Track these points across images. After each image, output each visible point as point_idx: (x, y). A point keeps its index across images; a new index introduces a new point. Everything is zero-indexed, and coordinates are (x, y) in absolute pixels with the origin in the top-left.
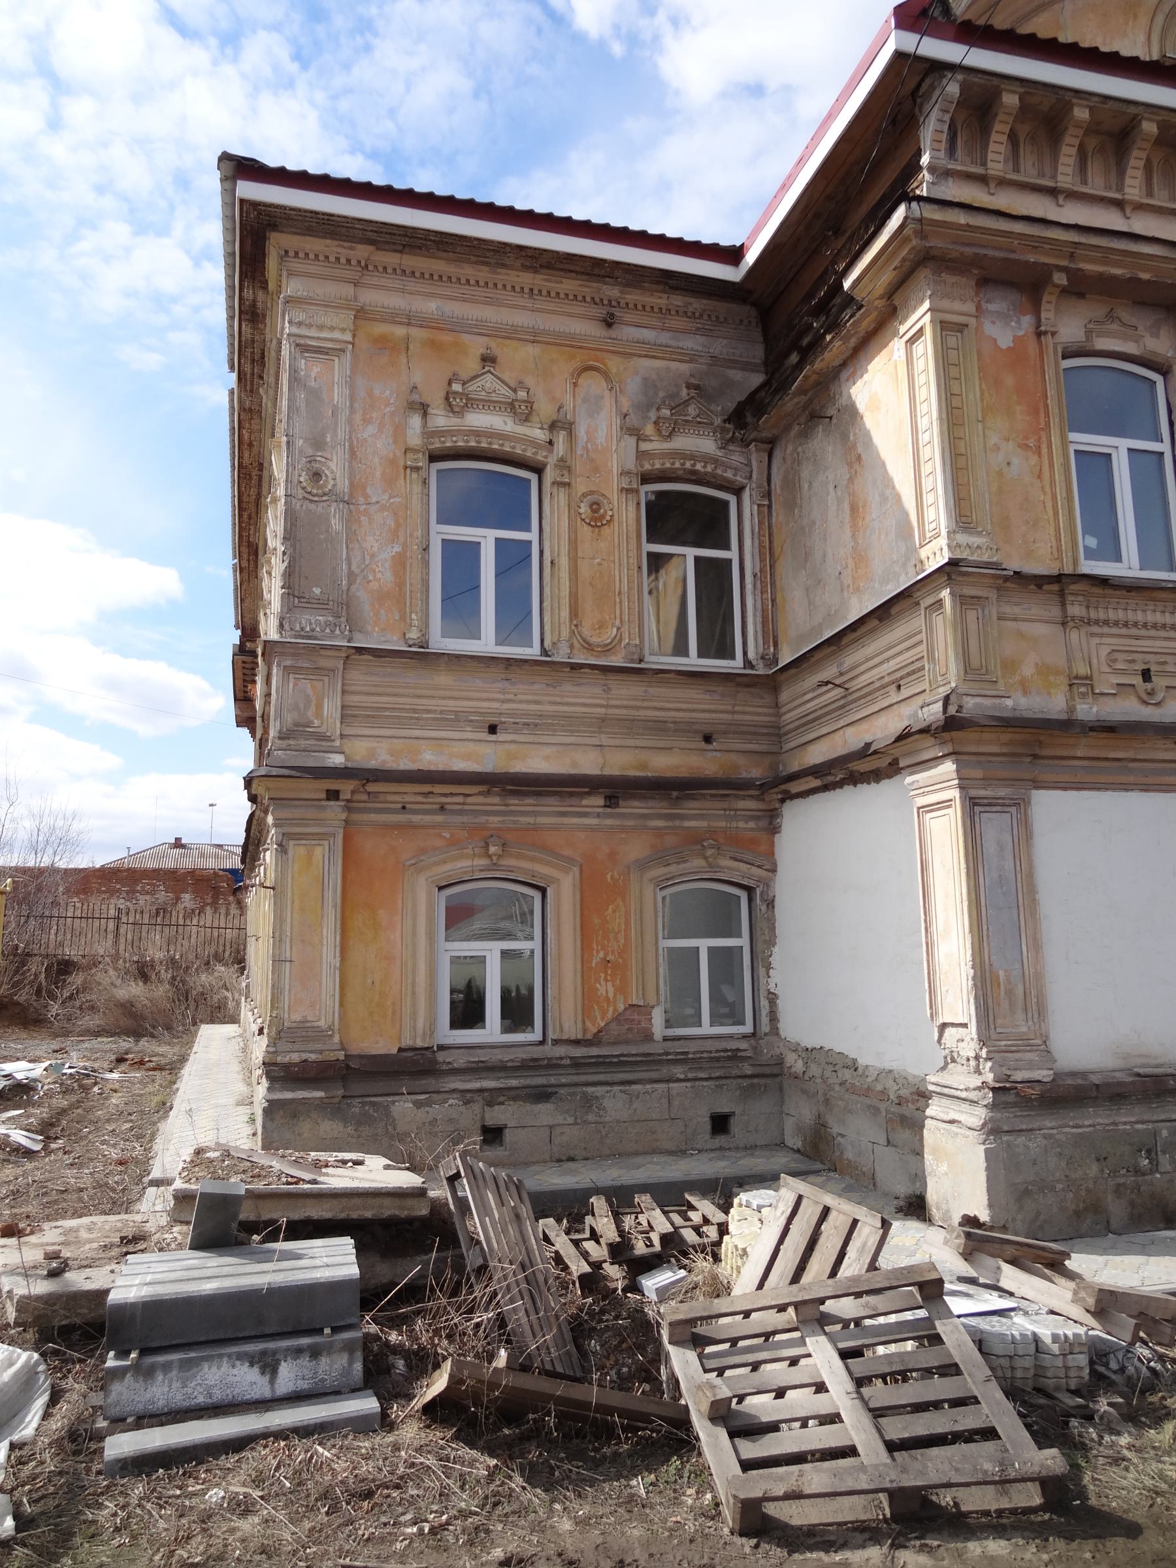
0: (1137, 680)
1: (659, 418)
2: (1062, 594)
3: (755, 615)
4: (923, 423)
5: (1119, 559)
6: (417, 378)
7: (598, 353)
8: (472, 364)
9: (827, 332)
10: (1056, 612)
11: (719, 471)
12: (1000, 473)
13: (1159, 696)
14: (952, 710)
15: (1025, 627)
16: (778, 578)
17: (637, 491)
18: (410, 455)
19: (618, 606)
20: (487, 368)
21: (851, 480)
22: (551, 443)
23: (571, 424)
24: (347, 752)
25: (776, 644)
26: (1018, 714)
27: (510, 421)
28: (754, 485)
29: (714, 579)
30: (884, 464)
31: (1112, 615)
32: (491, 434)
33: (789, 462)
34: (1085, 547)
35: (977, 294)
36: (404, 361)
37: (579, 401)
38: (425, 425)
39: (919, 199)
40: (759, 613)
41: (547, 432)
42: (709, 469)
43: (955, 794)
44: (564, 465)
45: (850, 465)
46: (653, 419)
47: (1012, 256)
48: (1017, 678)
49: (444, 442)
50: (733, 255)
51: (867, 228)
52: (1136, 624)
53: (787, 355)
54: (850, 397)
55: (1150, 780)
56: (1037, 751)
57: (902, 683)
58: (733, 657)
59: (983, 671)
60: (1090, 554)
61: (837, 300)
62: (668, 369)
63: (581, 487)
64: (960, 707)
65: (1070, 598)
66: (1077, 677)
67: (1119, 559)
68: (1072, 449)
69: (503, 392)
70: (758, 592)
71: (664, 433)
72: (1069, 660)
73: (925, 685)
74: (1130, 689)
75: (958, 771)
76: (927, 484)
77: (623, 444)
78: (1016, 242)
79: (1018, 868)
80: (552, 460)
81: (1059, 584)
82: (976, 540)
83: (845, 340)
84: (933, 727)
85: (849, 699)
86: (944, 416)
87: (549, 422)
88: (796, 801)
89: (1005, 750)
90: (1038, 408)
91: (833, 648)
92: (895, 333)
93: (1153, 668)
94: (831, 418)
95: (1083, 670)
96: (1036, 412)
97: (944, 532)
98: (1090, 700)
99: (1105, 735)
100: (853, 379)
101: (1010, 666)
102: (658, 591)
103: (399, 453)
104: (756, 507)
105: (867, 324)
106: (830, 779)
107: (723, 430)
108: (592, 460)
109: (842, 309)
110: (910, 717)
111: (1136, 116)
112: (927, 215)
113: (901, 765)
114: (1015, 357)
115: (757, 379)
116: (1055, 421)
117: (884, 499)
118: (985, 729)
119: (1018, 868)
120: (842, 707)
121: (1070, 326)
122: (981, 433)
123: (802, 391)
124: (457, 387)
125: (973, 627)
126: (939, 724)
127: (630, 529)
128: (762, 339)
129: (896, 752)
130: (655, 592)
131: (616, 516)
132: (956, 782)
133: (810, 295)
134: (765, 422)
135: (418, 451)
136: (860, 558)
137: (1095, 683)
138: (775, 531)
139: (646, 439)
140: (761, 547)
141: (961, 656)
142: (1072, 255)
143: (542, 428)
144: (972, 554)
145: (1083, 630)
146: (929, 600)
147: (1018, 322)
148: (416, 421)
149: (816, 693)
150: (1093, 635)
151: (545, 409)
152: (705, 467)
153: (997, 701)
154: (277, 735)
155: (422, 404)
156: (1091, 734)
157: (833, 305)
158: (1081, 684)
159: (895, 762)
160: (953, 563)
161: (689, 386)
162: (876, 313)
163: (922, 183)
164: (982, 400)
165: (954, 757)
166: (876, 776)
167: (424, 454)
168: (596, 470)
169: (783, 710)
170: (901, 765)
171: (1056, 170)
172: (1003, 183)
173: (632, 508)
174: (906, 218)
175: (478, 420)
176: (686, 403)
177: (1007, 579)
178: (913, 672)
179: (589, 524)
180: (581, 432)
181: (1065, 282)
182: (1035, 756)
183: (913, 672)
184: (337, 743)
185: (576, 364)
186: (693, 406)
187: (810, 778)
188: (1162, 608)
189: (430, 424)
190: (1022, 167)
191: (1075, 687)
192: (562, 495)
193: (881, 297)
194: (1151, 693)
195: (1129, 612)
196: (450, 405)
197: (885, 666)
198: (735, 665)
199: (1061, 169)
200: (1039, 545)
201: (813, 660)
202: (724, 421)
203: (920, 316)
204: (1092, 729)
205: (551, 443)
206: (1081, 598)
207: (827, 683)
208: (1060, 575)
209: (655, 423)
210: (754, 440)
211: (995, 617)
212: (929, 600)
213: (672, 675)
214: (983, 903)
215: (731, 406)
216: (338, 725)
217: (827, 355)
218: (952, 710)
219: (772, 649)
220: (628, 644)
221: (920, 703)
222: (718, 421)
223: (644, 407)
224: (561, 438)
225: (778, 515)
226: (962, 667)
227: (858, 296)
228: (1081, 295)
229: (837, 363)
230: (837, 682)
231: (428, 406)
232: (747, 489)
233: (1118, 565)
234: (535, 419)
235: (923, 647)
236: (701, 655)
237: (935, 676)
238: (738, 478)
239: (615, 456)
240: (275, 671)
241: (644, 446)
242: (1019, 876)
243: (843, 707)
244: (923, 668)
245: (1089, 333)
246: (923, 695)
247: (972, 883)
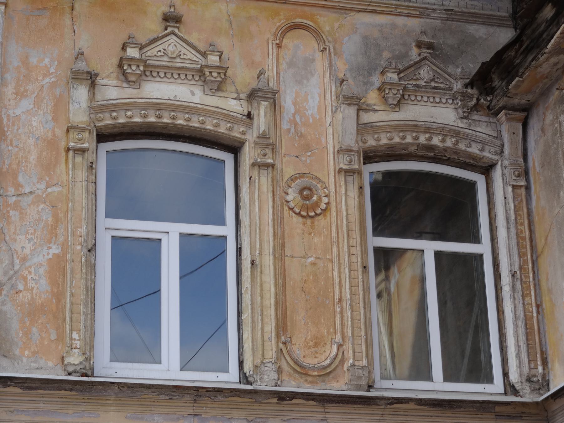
1: (384, 83)
3: (516, 326)
6: (84, 42)
7: (306, 9)
8: (152, 25)
11: (462, 146)
16: (543, 278)
17: (359, 172)
18: (73, 135)
19: (338, 316)
20: (169, 30)
22: (249, 116)
23: (275, 93)
25: (545, 362)
27: (198, 91)
28: (506, 163)
29: (462, 281)
32: (176, 107)
33: (549, 134)
36: (68, 22)
37: (284, 66)
38: (92, 97)
40: (521, 323)
41: (244, 103)
42: (449, 143)
44: (266, 142)
46: (377, 84)
49: (115, 118)
53: (540, 8)
58: (489, 379)
62: (394, 26)
63: (288, 171)
69: (190, 56)
70: (519, 295)
71: (391, 101)
77: (340, 115)
80: (251, 137)
87: (247, 91)
102: (389, 294)
103: (60, 132)
104: (510, 189)
107: (464, 96)
108: (301, 136)
115: (505, 36)
124: (132, 52)
127: (352, 219)
130: (385, 294)
131: (333, 204)
134: (517, 86)
135: (83, 130)
138: (536, 219)
139: (369, 109)
140: (519, 238)
143: (238, 99)
148: (81, 93)
151: (243, 77)
152: (443, 141)
155: (89, 73)
161: (419, 45)
167: (90, 132)
168: (307, 147)
173: (353, 193)
175: (158, 90)
176: (417, 64)
179: (299, 214)
180: (287, 102)
185: (280, 21)
186: (426, 69)
189: (98, 97)
192: (264, 179)
196: (124, 74)
198: (492, 390)
202: (466, 86)
205: (249, 116)
209: (379, 89)
210: (504, 108)
213: (411, 405)
215: (473, 68)
219: (540, 369)
220: (353, 365)
222: (458, 86)
223: (365, 71)
224: (262, 111)
225: (538, 198)
231: (96, 75)
232: (499, 167)
234: (230, 88)
236: (447, 378)
238: (486, 154)
239: (330, 130)
241: (367, 117)
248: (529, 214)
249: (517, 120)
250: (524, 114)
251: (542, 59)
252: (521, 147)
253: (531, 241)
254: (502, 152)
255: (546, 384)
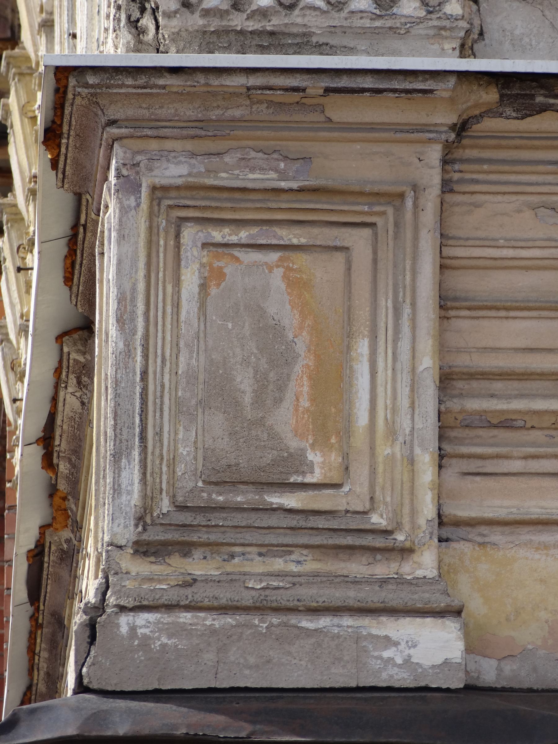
24: (476, 605)
154: (128, 534)
184: (426, 563)
216: (427, 473)
240: (110, 217)
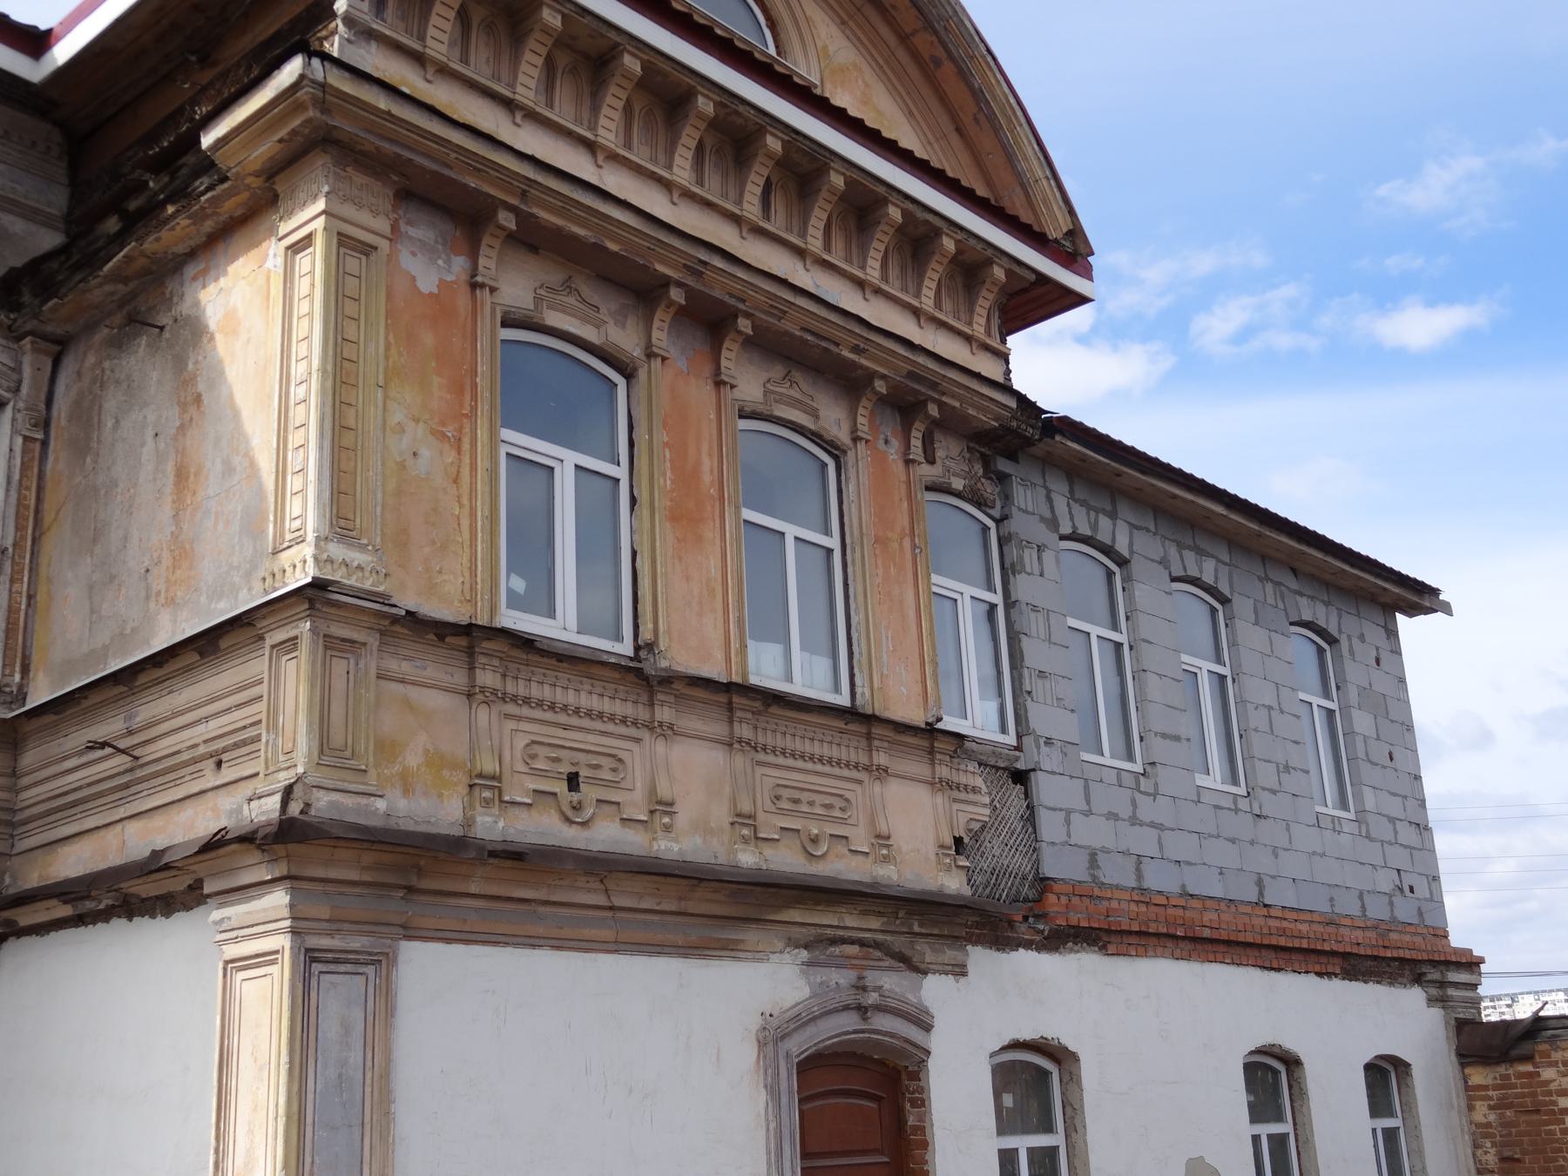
0: (561, 787)
2: (470, 653)
4: (298, 370)
5: (551, 613)
9: (170, 199)
10: (459, 678)
12: (402, 466)
13: (588, 812)
14: (295, 809)
15: (413, 693)
16: (43, 560)
21: (182, 429)
25: (25, 670)
26: (392, 824)
28: (21, 405)
30: (236, 414)
31: (535, 692)
34: (510, 591)
35: (395, 208)
39: (325, 57)
43: (283, 942)
45: (183, 406)
47: (446, 172)
48: (397, 768)
50: (35, 41)
51: (249, 69)
52: (565, 708)
53: (102, 216)
54: (197, 303)
55: (566, 933)
56: (414, 881)
57: (225, 757)
59: (348, 753)
60: (515, 602)
61: (190, 159)
64: (308, 805)
65: (482, 659)
66: (480, 776)
67: (551, 613)
68: (503, 450)
72: (472, 750)
73: (258, 765)
74: (551, 798)
75: (292, 906)
76: (294, 460)
78: (454, 155)
79: (369, 1063)
81: (468, 639)
82: (357, 557)
83: (198, 218)
84: (260, 834)
85: (138, 775)
86: (330, 368)
88: (26, 940)
89: (366, 877)
90: (462, 385)
91: (123, 689)
92: (272, 231)
93: (584, 773)
94: (162, 328)
95: (490, 766)
96: (460, 391)
97: (311, 537)
98: (496, 811)
99: (509, 863)
100: (203, 277)
101: (387, 749)
104: (19, 440)
105: (231, 207)
106: (89, 905)
109: (197, 174)
110: (231, 812)
111: (617, 45)
112: (332, 80)
113: (206, 890)
114: (439, 307)
115: (49, 240)
116: (483, 409)
117: (229, 470)
118: (342, 843)
119: (369, 1063)
120: (125, 787)
121: (517, 285)
122: (380, 404)
123: (118, 277)
125: (339, 684)
126: (269, 829)
128: (65, 180)
129: (200, 869)
132: (288, 923)
133: (152, 137)
134: (54, 310)
136: (182, 553)
137: (505, 786)
138: (49, 485)
141: (316, 727)
142: (524, 194)
144: (349, 575)
145: (496, 709)
146: (280, 636)
147: (448, 262)
149: (84, 759)
150: (508, 716)
153: (364, 801)
156: (491, 861)
157: (182, 164)
158: (486, 785)
159: (196, 886)
160: (318, 585)
162: (245, 195)
163: (334, 32)
164: (387, 358)
165: (288, 884)
166: (165, 905)
169: (25, 781)
170: (206, 890)
171: (516, 78)
172: (444, 71)
174: (302, 77)
177: (395, 620)
178: (244, 743)
181: (513, 227)
182: (410, 890)
183: (244, 743)
187: (54, 902)
188: (599, 690)
190: (472, 59)
191: (477, 789)
193: (257, 174)
194: (577, 808)
195: (559, 690)
197: (201, 728)
199: (521, 78)
200: (446, 577)
201: (85, 704)
203: (308, 216)
204: (493, 854)
206: (496, 662)
207: (103, 745)
208: (471, 625)
211: (373, 672)
212: (280, 636)
214: (309, 1120)
217: (165, 234)
218: (295, 809)
219: (17, 677)
221: (249, 793)
225: (57, 460)
226: (316, 744)
227: (223, 160)
228: (533, 249)
229: (180, 249)
230: (122, 744)
232: (9, 409)
233: (550, 622)
235: (262, 706)
237: (275, 752)
242: (369, 1075)
243: (127, 786)
244: (257, 739)
245: (538, 300)
246: (254, 780)
247: (296, 1088)
248: (41, 476)
249: (46, 353)
250: (57, 348)
251: (94, 282)
252: (45, 389)
253: (37, 511)
254: (17, 390)
255: (22, 697)
